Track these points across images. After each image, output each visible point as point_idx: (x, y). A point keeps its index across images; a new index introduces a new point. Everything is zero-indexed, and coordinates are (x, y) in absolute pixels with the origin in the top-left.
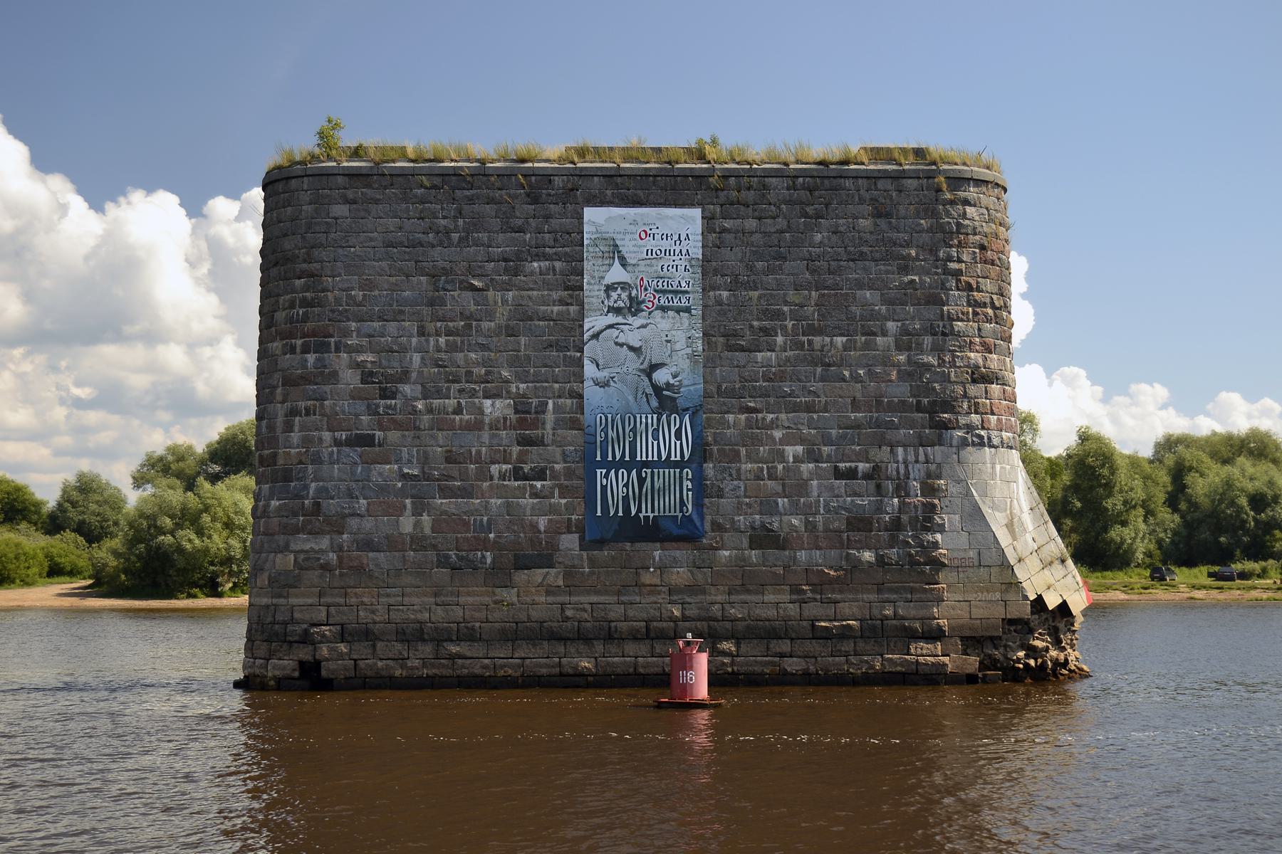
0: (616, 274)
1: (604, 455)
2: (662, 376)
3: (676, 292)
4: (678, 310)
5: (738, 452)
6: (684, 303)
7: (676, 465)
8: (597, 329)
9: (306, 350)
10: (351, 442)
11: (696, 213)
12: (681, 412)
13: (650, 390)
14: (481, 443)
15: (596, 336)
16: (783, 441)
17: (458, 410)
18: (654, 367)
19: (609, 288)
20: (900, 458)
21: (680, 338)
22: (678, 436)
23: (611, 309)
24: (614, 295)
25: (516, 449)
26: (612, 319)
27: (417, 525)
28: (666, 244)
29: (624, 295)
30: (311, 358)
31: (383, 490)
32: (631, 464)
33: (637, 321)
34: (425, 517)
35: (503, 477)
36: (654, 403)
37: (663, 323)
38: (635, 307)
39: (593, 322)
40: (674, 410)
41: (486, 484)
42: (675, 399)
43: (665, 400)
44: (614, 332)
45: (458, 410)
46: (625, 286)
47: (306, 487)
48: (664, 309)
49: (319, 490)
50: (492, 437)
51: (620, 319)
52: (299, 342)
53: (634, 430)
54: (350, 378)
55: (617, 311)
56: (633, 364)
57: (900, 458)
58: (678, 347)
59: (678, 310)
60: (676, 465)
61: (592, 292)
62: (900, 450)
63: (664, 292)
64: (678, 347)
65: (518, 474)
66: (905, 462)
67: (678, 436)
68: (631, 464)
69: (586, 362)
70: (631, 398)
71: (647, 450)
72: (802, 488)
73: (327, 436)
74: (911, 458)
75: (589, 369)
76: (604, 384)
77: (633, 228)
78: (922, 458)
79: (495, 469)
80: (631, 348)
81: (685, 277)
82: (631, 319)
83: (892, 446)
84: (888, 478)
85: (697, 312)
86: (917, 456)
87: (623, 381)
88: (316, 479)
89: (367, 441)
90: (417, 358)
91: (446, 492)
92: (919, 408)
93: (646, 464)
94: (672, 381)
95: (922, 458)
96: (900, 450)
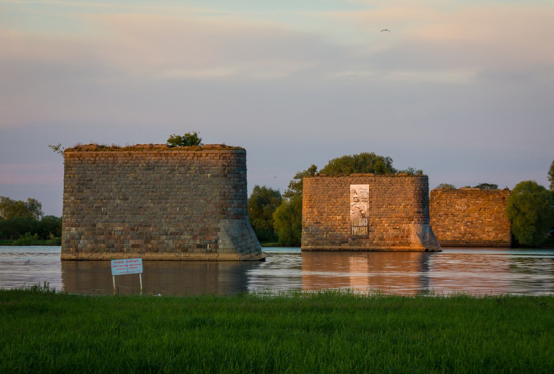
0: (355, 196)
1: (353, 225)
2: (363, 212)
3: (365, 198)
4: (365, 201)
5: (377, 225)
6: (366, 200)
7: (365, 226)
8: (352, 205)
9: (309, 208)
10: (316, 223)
11: (368, 185)
12: (366, 218)
13: (361, 214)
14: (337, 223)
15: (352, 206)
16: (385, 223)
17: (333, 218)
18: (361, 211)
19: (354, 198)
20: (404, 226)
21: (366, 206)
22: (365, 222)
23: (354, 201)
24: (355, 199)
25: (342, 224)
26: (355, 203)
27: (326, 236)
28: (363, 191)
29: (357, 199)
30: (310, 209)
31: (322, 231)
32: (358, 226)
33: (359, 203)
34: (328, 235)
35: (340, 229)
36: (361, 217)
37: (363, 203)
38: (358, 201)
39: (352, 203)
40: (365, 218)
41: (337, 230)
42: (365, 216)
43: (363, 216)
44: (355, 205)
45: (333, 218)
46: (357, 198)
47: (309, 230)
48: (363, 201)
49: (311, 231)
50: (338, 222)
51: (356, 203)
52: (308, 207)
53: (358, 221)
54: (316, 213)
55: (356, 202)
56: (358, 210)
57: (404, 226)
58: (365, 207)
59: (365, 201)
60: (365, 226)
61: (352, 199)
62: (404, 225)
63: (363, 198)
64: (365, 207)
65: (341, 228)
66: (405, 226)
67: (365, 222)
68: (358, 226)
69: (351, 210)
70: (358, 216)
71: (360, 224)
72: (387, 231)
73: (312, 222)
74: (406, 226)
75: (351, 211)
76: (354, 214)
77: (358, 188)
78: (407, 226)
79: (338, 227)
80: (358, 208)
81: (366, 196)
82: (358, 203)
83: (403, 224)
84: (401, 229)
85: (368, 202)
86: (406, 226)
87: (356, 213)
88: (311, 229)
89: (319, 223)
90: (326, 209)
91: (331, 231)
92: (407, 218)
93: (360, 226)
94: (364, 213)
95: (407, 226)
96: (404, 225)
